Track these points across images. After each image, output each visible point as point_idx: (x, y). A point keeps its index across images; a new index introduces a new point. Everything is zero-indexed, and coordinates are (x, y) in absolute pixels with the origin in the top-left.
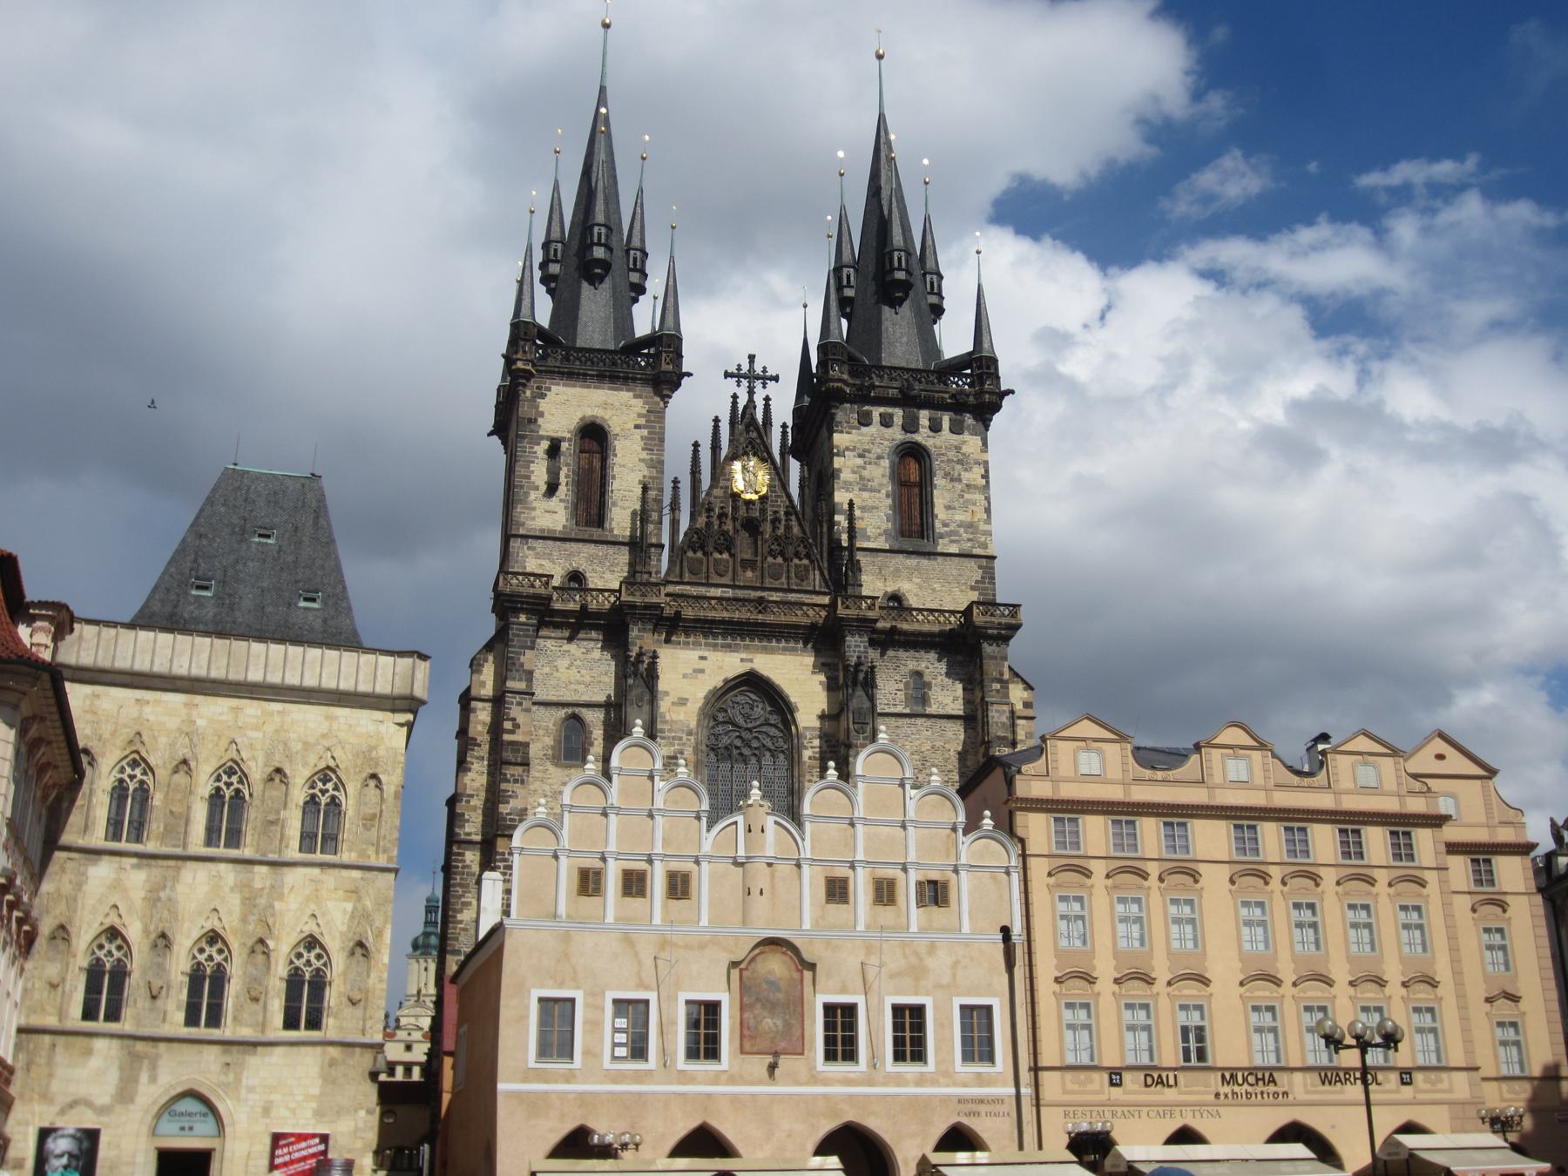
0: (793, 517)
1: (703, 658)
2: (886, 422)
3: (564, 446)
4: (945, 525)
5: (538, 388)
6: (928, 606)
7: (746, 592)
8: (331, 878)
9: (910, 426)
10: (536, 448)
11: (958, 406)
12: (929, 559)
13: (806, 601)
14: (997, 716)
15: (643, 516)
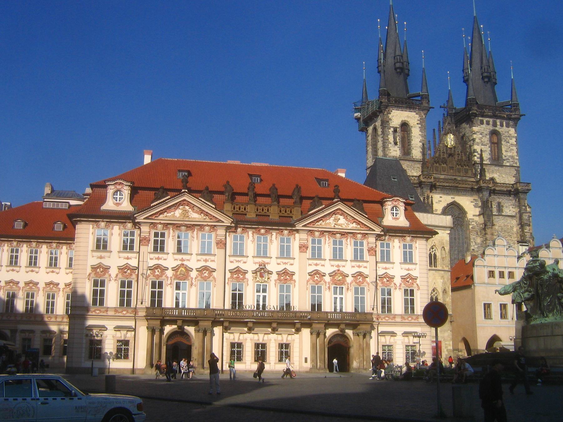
0: (463, 153)
1: (441, 197)
2: (488, 123)
3: (398, 129)
4: (505, 157)
5: (389, 111)
6: (502, 182)
7: (451, 176)
8: (437, 274)
9: (495, 125)
10: (389, 130)
11: (509, 118)
12: (501, 167)
13: (468, 180)
14: (525, 217)
15: (424, 154)
